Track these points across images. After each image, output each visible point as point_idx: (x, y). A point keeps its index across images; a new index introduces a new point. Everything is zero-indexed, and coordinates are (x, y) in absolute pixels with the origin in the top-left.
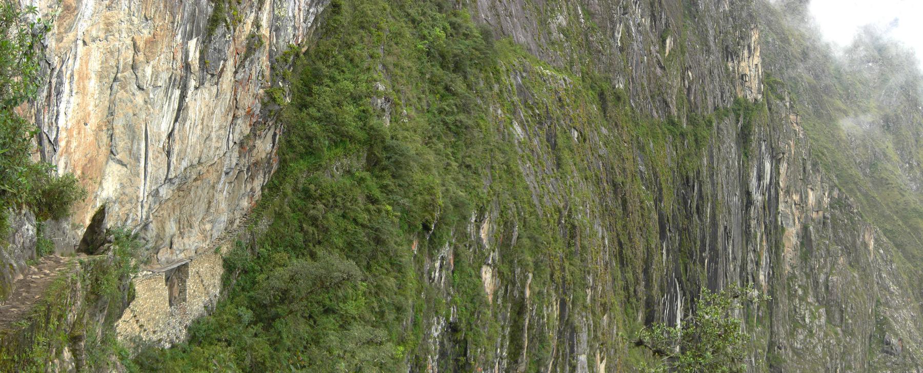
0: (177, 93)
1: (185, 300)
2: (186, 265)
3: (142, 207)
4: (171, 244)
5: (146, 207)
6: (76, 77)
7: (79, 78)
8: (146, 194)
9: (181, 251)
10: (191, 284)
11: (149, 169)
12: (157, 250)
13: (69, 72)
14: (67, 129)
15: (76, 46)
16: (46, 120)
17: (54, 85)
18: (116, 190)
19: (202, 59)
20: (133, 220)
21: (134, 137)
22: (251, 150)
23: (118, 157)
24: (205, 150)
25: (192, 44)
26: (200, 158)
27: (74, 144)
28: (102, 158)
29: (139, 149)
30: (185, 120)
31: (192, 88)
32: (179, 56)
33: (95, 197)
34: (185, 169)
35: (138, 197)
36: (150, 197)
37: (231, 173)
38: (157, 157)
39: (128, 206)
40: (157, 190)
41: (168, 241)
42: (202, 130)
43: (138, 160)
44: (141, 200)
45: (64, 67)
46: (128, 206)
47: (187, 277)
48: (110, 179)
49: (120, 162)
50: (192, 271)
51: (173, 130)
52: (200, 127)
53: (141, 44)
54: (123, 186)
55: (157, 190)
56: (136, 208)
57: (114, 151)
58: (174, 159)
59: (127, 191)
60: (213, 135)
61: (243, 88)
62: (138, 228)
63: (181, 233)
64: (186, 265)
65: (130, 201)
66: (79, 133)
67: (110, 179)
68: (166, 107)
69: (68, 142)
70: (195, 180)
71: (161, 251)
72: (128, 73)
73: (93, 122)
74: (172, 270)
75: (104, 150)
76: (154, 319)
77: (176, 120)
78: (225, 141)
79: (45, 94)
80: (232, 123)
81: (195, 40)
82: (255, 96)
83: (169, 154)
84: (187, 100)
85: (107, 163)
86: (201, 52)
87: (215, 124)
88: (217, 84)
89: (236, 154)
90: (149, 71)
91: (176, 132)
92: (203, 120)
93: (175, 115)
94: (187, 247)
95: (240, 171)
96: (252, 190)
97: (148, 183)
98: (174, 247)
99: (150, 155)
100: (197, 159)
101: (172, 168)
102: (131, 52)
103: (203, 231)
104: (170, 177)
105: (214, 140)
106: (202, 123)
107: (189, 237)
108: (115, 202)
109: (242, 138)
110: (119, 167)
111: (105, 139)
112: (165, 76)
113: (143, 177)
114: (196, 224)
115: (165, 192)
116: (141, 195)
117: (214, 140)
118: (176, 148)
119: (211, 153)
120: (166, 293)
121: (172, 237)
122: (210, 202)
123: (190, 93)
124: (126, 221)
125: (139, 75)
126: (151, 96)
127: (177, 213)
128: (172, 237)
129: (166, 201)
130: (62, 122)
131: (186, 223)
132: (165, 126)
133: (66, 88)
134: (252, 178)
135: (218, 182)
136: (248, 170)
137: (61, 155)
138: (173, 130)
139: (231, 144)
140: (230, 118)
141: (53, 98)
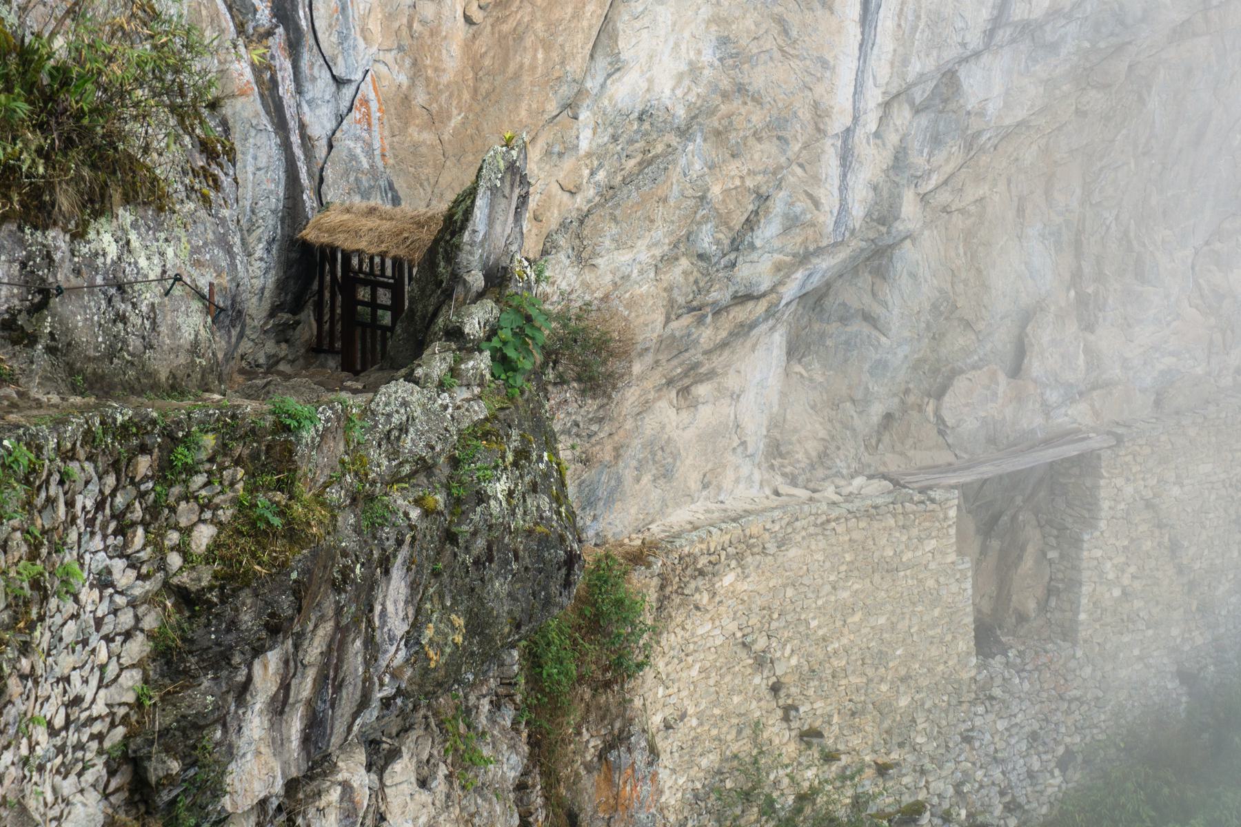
1: (1068, 632)
2: (1086, 464)
3: (846, 159)
4: (1021, 351)
5: (872, 163)
8: (873, 97)
9: (1073, 394)
10: (1108, 561)
12: (938, 379)
18: (694, 70)
20: (792, 223)
33: (571, 107)
35: (820, 113)
36: (902, 116)
39: (763, 154)
40: (949, 81)
44: (839, 122)
46: (763, 154)
47: (1090, 522)
50: (1115, 490)
55: (949, 81)
56: (809, 161)
59: (758, 79)
62: (825, 265)
63: (1082, 301)
64: (1086, 464)
65: (777, 129)
71: (960, 384)
74: (1014, 481)
76: (882, 709)
98: (1035, 367)
108: (684, 133)
116: (841, 101)
120: (961, 593)
121: (1027, 317)
124: (750, 224)
128: (1027, 317)
129: (1007, 135)
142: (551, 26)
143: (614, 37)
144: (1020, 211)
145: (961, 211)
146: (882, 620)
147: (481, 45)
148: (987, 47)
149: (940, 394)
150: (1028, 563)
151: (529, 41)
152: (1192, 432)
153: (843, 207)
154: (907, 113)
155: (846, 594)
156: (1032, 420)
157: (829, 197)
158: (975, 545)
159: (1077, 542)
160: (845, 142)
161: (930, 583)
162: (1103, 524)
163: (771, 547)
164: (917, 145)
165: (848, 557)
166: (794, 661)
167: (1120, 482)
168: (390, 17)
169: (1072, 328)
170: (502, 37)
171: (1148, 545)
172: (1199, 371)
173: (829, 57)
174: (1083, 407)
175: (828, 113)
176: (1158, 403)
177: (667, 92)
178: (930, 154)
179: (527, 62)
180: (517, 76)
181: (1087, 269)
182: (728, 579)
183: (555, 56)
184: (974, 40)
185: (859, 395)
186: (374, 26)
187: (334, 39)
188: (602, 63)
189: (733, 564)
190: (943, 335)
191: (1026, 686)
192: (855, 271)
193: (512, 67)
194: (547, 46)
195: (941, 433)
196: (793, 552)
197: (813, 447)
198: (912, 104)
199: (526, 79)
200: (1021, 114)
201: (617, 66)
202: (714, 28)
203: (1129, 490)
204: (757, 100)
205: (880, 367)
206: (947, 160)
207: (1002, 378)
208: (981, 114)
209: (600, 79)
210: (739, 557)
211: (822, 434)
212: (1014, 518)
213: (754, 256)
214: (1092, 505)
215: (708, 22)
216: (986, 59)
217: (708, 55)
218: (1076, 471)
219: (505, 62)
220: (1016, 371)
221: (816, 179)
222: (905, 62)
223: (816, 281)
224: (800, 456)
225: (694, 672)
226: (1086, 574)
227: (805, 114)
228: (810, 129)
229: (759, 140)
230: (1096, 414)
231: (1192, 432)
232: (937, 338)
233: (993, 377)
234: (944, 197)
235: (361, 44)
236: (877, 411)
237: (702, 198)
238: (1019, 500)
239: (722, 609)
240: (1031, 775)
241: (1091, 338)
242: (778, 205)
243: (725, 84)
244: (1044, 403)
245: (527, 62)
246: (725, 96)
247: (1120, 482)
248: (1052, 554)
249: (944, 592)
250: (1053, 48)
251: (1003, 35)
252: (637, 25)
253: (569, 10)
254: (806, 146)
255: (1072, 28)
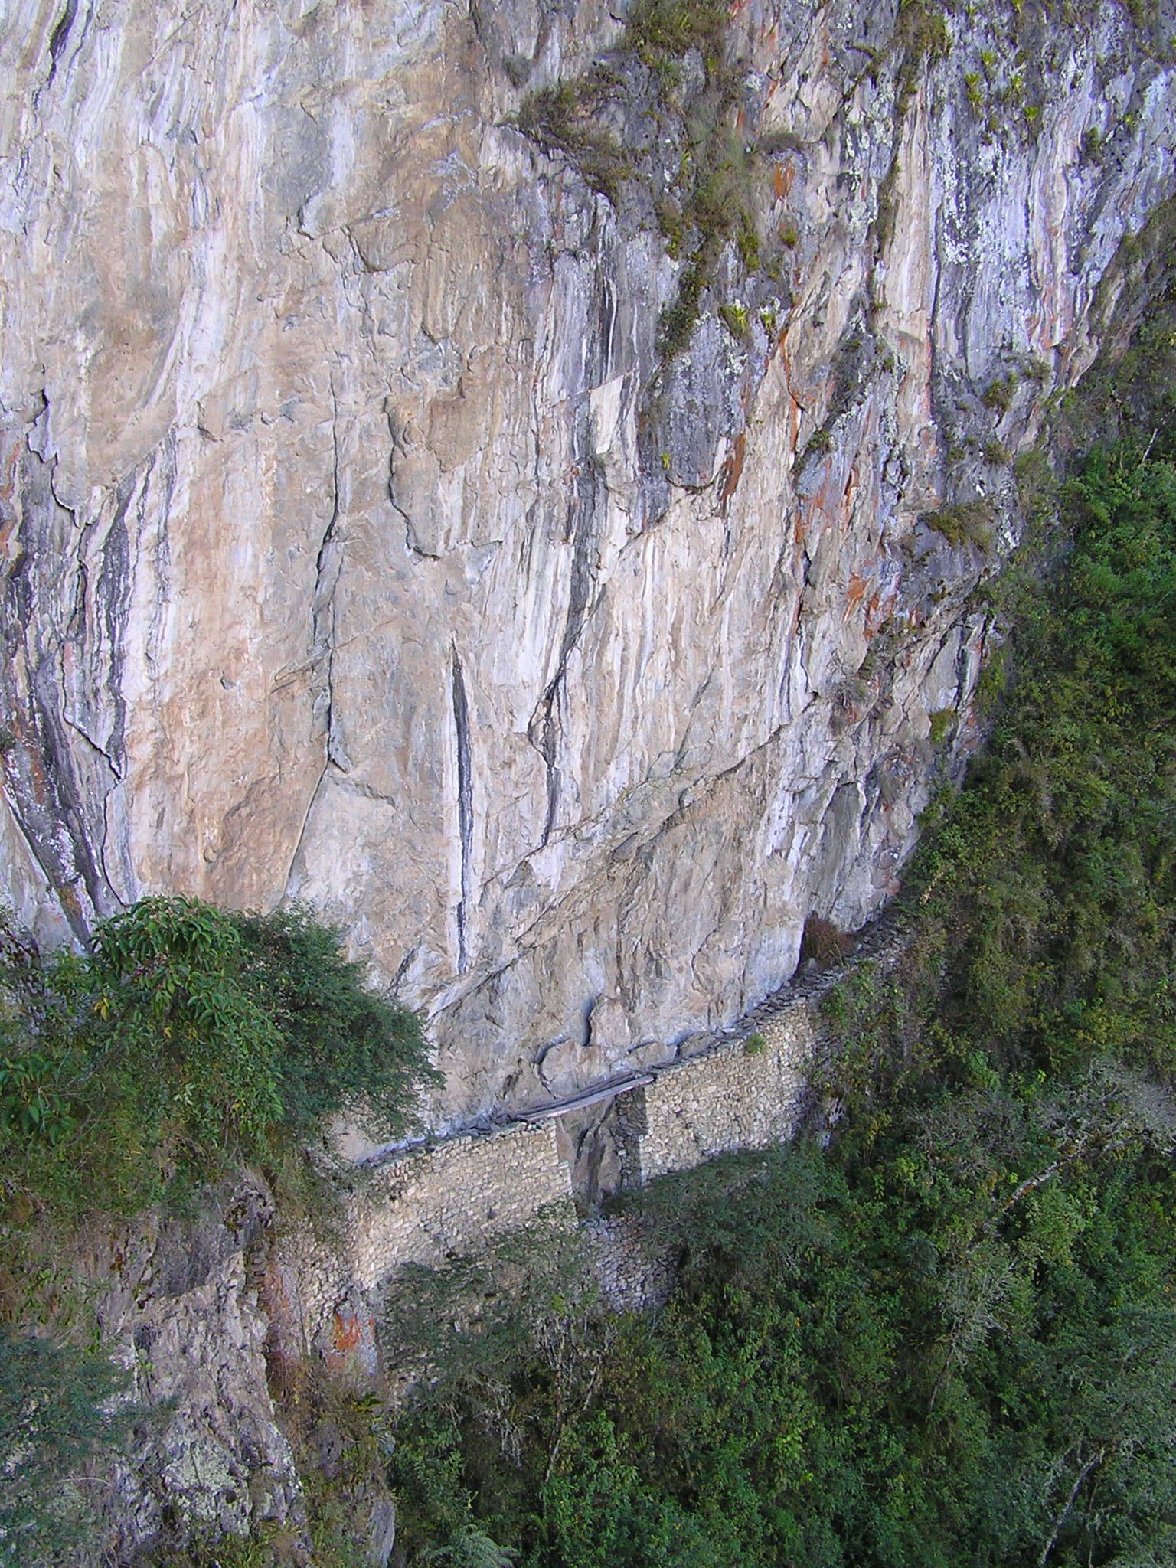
0: (563, 557)
2: (637, 1094)
4: (589, 1029)
6: (177, 545)
7: (190, 546)
8: (475, 883)
11: (479, 804)
13: (152, 530)
14: (156, 707)
15: (172, 444)
16: (74, 683)
17: (94, 575)
18: (357, 876)
19: (645, 440)
21: (413, 709)
22: (876, 716)
23: (355, 774)
24: (697, 728)
25: (607, 399)
26: (680, 754)
27: (185, 749)
28: (296, 784)
29: (433, 745)
30: (601, 641)
31: (619, 538)
32: (560, 443)
34: (626, 793)
35: (441, 897)
37: (812, 794)
38: (508, 764)
39: (408, 923)
41: (575, 1024)
42: (676, 665)
43: (432, 777)
45: (130, 515)
47: (643, 1131)
48: (335, 846)
49: (367, 790)
51: (561, 674)
52: (663, 657)
53: (414, 417)
54: (382, 865)
56: (438, 924)
57: (339, 757)
58: (571, 762)
59: (399, 879)
60: (725, 677)
61: (830, 516)
62: (457, 989)
66: (202, 714)
67: (335, 846)
68: (527, 604)
69: (163, 746)
70: (669, 824)
71: (552, 1052)
72: (379, 510)
73: (255, 674)
74: (595, 1108)
75: (302, 755)
77: (569, 643)
78: (772, 693)
79: (68, 603)
80: (797, 631)
81: (615, 386)
82: (880, 540)
83: (550, 753)
84: (603, 576)
85: (319, 791)
86: (642, 417)
87: (729, 640)
88: (723, 514)
89: (819, 729)
90: (451, 498)
91: (572, 678)
92: (675, 630)
93: (562, 627)
94: (650, 1035)
95: (845, 786)
96: (885, 842)
97: (478, 852)
98: (598, 1038)
99: (479, 755)
100: (670, 758)
101: (567, 794)
102: (382, 448)
103: (707, 984)
104: (560, 820)
105: (729, 693)
106: (675, 644)
107: (655, 1005)
109: (838, 677)
110: (363, 803)
111: (304, 723)
112: (513, 508)
113: (456, 831)
114: (679, 962)
115: (549, 867)
117: (729, 693)
118: (576, 733)
119: (722, 735)
121: (591, 1006)
122: (725, 892)
123: (609, 554)
124: (404, 968)
125: (417, 511)
126: (469, 573)
127: (609, 931)
128: (591, 1006)
130: (135, 683)
131: (641, 961)
132: (524, 657)
133: (142, 584)
134: (886, 802)
135: (752, 826)
136: (872, 777)
137: (139, 787)
138: (561, 674)
139: (800, 699)
140: (787, 617)
141: (98, 617)
142: (261, 860)
143: (303, 862)
144: (580, 941)
145: (544, 947)
146: (514, 1206)
147: (216, 875)
148: (545, 844)
149: (540, 1062)
150: (607, 1160)
151: (246, 870)
152: (701, 1068)
153: (462, 948)
154: (498, 889)
155: (489, 1192)
156: (600, 1071)
157: (452, 945)
158: (573, 1151)
159: (636, 1144)
160: (459, 911)
161: (543, 1179)
162: (650, 1132)
163: (437, 1168)
164: (508, 908)
165: (488, 1169)
166: (460, 1238)
167: (659, 1103)
168: (155, 864)
169: (619, 1010)
170: (230, 869)
171: (680, 1141)
172: (704, 1029)
173: (443, 860)
174: (632, 1058)
175: (446, 894)
176: (679, 1052)
177: (341, 892)
178: (518, 913)
179: (246, 882)
180: (241, 892)
181: (626, 974)
182: (411, 1191)
183: (264, 876)
184: (538, 841)
185: (489, 1066)
186: (146, 870)
187: (120, 880)
188: (296, 878)
189: (413, 1181)
190: (538, 1024)
191: (613, 1236)
192: (479, 989)
193: (236, 889)
194: (259, 872)
195: (544, 1084)
196: (451, 1170)
197: (462, 1101)
198: (501, 883)
199: (247, 893)
200: (573, 882)
201: (307, 879)
202: (367, 850)
203: (665, 1107)
204: (399, 891)
205: (501, 1047)
206: (529, 915)
207: (579, 1048)
208: (547, 885)
209: (296, 889)
210: (418, 1176)
211: (468, 1092)
212: (596, 1133)
213: (408, 987)
214: (642, 1118)
215: (363, 847)
216: (546, 850)
217: (365, 866)
218: (630, 1099)
219: (233, 884)
220: (587, 1042)
221: (443, 936)
222: (493, 859)
223: (452, 999)
224: (456, 1108)
225: (394, 1252)
226: (642, 1164)
227: (431, 897)
228: (436, 905)
229: (404, 915)
230: (641, 1063)
231: (701, 1068)
232: (535, 1026)
233: (572, 1047)
234: (530, 939)
235: (138, 882)
236: (501, 1074)
237: (370, 955)
238: (598, 1122)
239: (409, 1210)
240: (621, 1291)
241: (633, 1016)
242: (421, 954)
243: (378, 883)
244: (607, 1059)
245: (246, 882)
246: (379, 890)
247: (659, 1103)
248: (621, 1153)
249: (552, 1184)
250: (589, 840)
251: (552, 836)
252: (318, 852)
253: (272, 848)
254: (434, 916)
255: (599, 827)
